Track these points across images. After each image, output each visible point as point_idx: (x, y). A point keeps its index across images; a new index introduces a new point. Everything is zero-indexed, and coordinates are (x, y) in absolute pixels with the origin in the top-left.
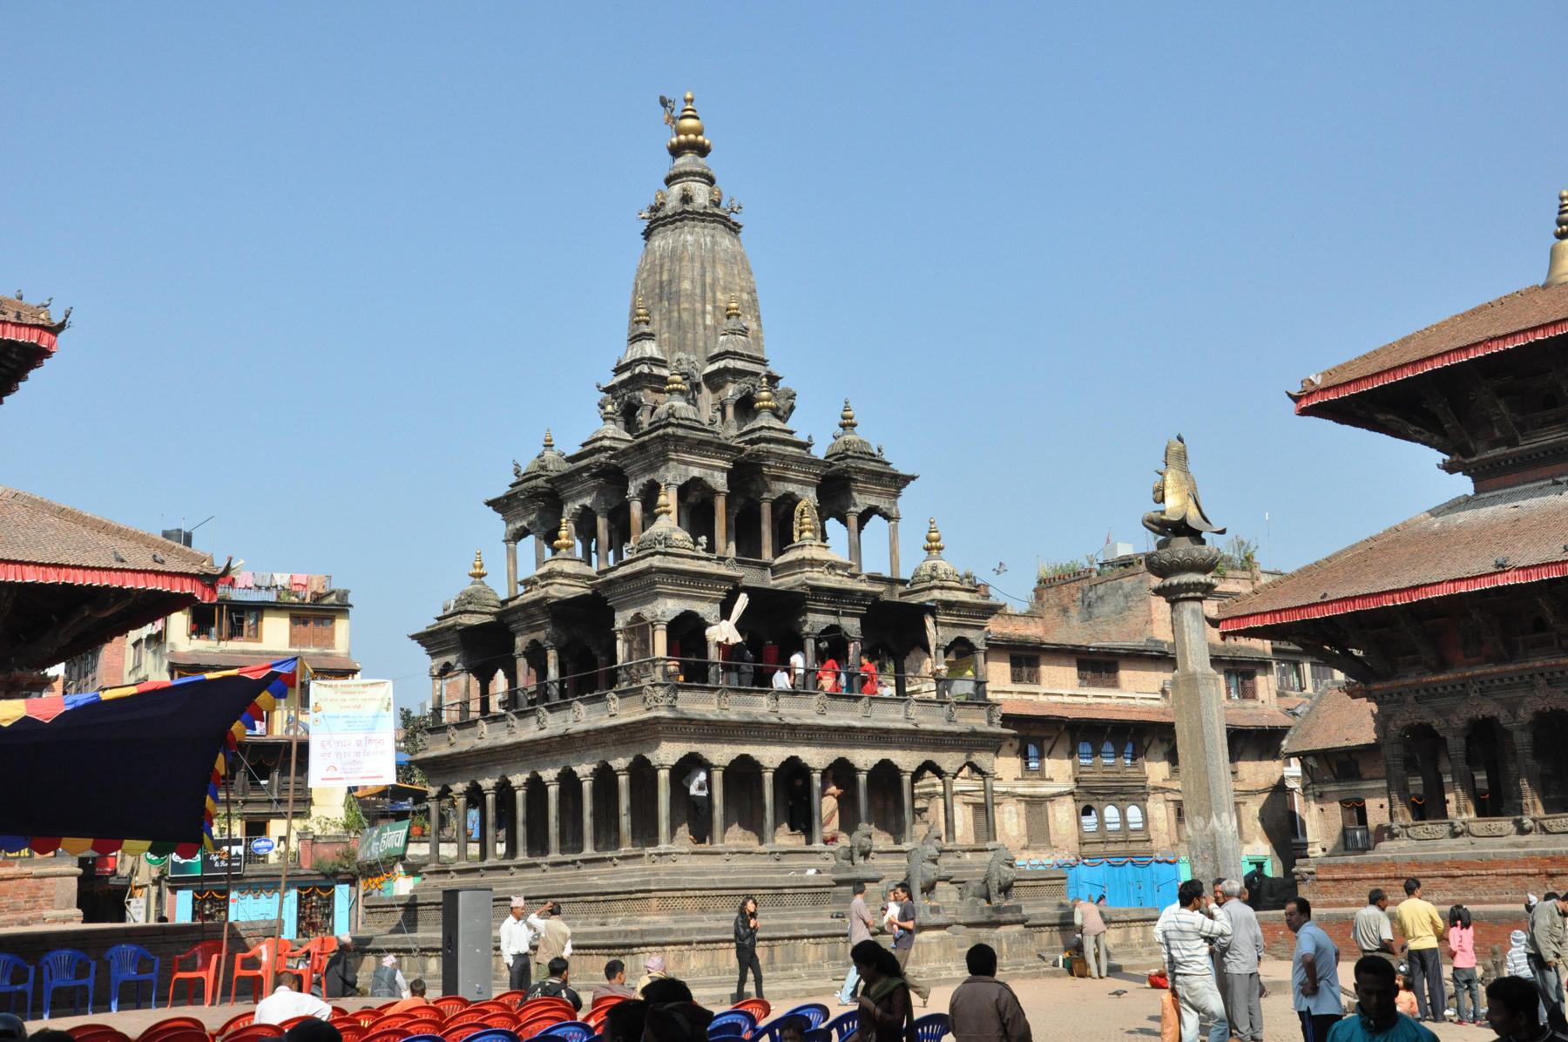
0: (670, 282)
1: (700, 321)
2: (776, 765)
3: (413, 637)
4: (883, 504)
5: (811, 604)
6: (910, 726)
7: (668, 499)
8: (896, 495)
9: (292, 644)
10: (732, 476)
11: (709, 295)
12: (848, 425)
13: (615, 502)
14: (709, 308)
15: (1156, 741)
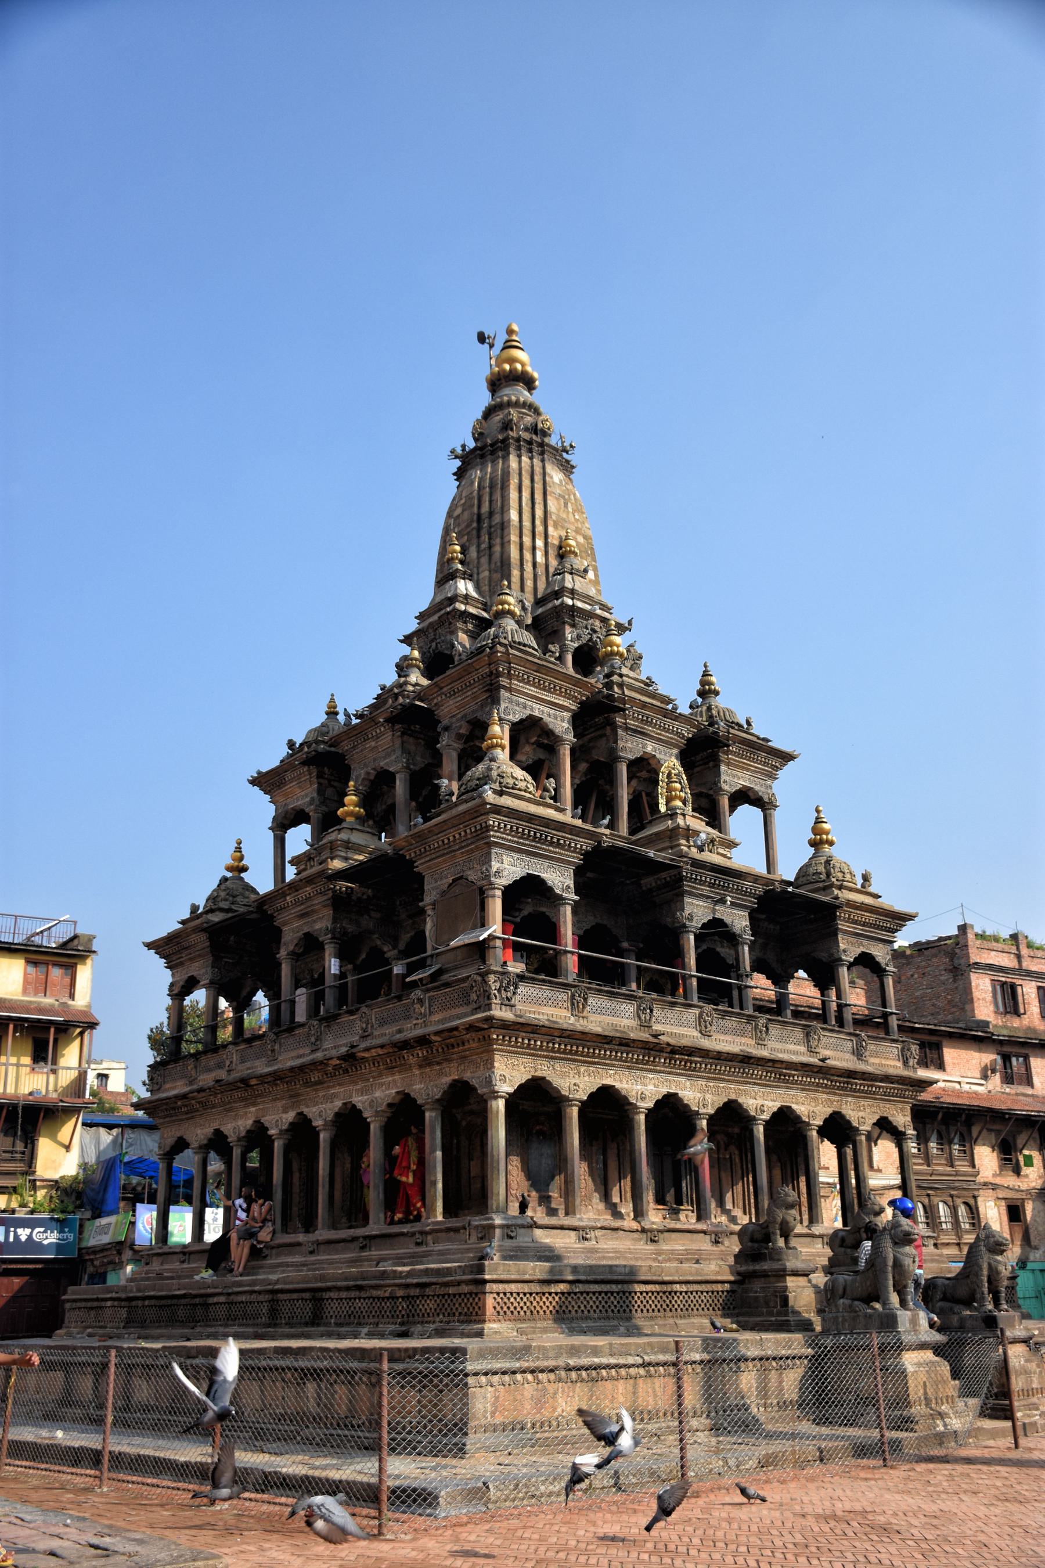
0: (491, 514)
1: (528, 556)
2: (651, 1105)
3: (149, 946)
4: (757, 785)
5: (687, 886)
6: (814, 1060)
7: (500, 732)
8: (773, 777)
9: (25, 991)
10: (579, 720)
11: (540, 528)
12: (706, 691)
13: (420, 762)
14: (540, 543)
15: (985, 1132)
